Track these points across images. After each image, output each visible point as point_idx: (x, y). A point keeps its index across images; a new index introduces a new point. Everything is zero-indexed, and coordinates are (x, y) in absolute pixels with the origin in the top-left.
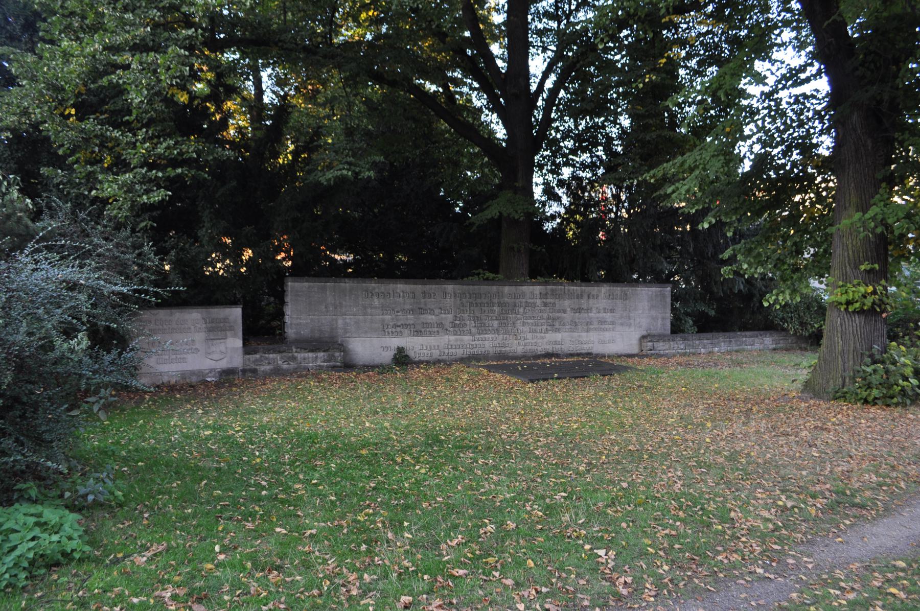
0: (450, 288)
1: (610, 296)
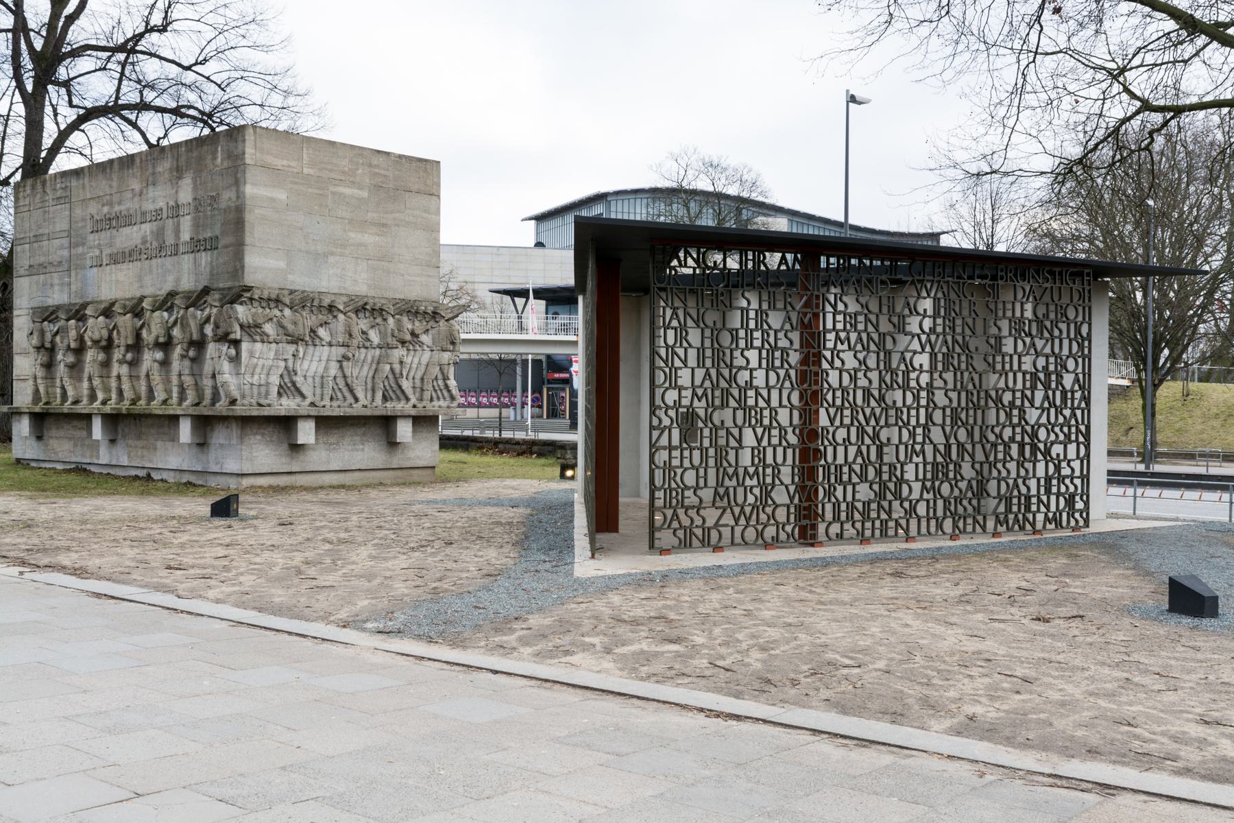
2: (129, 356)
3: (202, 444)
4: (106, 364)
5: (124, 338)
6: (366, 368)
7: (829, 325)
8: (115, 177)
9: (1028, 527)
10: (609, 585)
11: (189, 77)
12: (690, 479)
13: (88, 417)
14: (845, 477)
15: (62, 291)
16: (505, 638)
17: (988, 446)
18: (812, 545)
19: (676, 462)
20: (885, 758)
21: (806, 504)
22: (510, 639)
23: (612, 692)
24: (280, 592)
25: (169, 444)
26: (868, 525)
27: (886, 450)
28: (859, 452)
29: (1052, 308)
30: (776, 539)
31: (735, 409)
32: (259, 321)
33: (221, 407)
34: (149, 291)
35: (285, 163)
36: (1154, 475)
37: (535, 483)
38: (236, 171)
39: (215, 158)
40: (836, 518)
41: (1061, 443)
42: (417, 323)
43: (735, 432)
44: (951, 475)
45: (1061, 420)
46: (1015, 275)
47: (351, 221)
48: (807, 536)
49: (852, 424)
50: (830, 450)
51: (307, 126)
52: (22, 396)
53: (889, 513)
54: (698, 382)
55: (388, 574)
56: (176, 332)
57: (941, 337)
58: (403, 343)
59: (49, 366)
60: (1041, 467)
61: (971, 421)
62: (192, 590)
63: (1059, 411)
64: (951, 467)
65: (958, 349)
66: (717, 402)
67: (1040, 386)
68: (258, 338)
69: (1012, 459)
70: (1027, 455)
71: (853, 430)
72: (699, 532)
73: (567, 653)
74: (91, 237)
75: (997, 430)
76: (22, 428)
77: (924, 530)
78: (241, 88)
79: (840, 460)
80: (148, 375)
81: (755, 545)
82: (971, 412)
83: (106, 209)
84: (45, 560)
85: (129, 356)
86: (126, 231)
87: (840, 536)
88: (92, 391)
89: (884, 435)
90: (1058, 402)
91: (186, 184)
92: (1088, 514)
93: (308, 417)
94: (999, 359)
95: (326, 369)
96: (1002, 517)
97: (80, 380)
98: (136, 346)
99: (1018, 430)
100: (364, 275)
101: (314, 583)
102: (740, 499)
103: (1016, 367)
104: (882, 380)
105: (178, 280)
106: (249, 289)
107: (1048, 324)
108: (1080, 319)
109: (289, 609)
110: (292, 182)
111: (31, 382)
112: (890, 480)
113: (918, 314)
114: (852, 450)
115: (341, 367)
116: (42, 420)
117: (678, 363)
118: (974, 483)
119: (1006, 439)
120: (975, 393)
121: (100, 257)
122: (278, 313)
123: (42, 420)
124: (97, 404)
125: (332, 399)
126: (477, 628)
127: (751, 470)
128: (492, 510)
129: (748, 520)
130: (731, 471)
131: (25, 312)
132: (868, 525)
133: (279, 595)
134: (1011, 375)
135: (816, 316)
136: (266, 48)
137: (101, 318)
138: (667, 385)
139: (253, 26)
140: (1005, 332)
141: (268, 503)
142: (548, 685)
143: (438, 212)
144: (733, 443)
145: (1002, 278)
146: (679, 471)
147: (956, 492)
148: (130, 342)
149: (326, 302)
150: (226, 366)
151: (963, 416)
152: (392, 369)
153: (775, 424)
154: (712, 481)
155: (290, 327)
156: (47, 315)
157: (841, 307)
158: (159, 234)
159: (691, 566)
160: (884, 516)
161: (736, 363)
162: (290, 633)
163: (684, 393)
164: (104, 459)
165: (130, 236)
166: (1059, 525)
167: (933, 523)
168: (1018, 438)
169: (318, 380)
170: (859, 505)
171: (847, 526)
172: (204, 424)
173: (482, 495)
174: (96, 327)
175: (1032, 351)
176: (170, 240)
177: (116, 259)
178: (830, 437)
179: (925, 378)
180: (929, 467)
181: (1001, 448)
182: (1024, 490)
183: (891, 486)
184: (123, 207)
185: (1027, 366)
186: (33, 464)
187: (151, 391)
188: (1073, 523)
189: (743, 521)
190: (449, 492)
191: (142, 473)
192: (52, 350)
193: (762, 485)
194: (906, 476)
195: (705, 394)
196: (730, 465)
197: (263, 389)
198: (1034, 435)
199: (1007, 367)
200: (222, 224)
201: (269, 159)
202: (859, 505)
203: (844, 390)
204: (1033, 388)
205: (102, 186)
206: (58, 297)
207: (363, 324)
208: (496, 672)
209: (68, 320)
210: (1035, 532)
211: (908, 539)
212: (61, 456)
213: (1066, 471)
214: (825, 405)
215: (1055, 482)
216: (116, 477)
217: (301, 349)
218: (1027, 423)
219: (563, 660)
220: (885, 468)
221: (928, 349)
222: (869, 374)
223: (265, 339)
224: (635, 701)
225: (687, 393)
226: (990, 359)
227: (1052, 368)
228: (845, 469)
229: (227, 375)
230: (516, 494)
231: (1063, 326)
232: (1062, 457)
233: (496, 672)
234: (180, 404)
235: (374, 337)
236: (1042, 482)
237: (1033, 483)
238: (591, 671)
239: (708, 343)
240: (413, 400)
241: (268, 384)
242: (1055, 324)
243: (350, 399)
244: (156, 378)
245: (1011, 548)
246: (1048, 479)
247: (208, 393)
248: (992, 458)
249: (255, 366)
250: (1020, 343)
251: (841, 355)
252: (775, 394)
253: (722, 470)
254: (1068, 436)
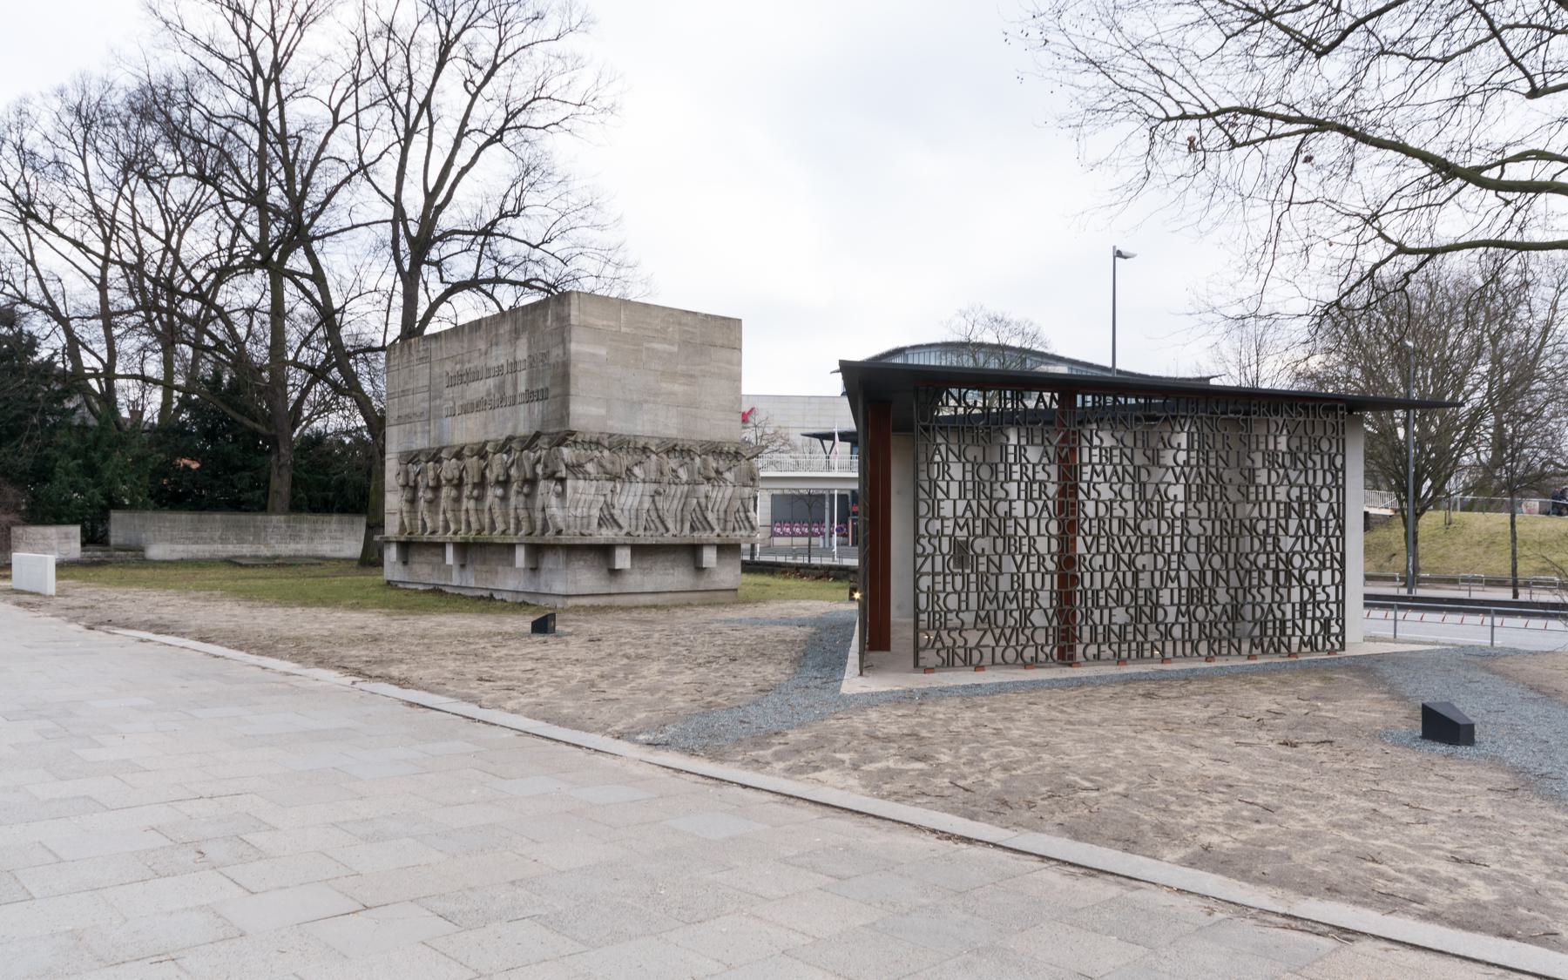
0: (218, 516)
1: (340, 522)
2: (475, 493)
3: (534, 569)
4: (458, 500)
5: (471, 478)
6: (676, 502)
7: (1086, 459)
8: (466, 339)
9: (1283, 649)
10: (871, 701)
11: (537, 254)
12: (952, 602)
13: (442, 545)
14: (1102, 602)
15: (423, 438)
16: (761, 753)
17: (1242, 573)
18: (1070, 665)
19: (939, 587)
20: (1112, 890)
21: (1064, 627)
22: (766, 754)
23: (851, 810)
24: (570, 704)
25: (508, 569)
26: (1124, 647)
27: (1141, 576)
28: (1115, 577)
29: (1306, 440)
30: (1035, 659)
31: (995, 538)
32: (583, 461)
33: (550, 537)
34: (492, 436)
35: (605, 323)
36: (1415, 599)
37: (826, 604)
38: (563, 331)
39: (546, 321)
40: (1093, 640)
41: (1315, 569)
42: (721, 462)
43: (996, 559)
44: (1206, 600)
45: (1315, 547)
46: (1269, 411)
47: (663, 373)
48: (1066, 656)
49: (1108, 551)
50: (1087, 577)
51: (636, 294)
52: (392, 528)
53: (1145, 636)
54: (959, 512)
55: (670, 688)
56: (513, 471)
57: (1195, 469)
58: (709, 479)
59: (413, 501)
60: (1295, 595)
61: (1225, 548)
62: (494, 701)
63: (1313, 539)
64: (1206, 592)
65: (1212, 481)
66: (979, 531)
67: (1294, 515)
68: (581, 476)
69: (1266, 585)
70: (1282, 580)
71: (1110, 558)
72: (961, 652)
73: (817, 769)
74: (447, 391)
75: (1252, 557)
76: (391, 554)
77: (1179, 651)
78: (580, 262)
79: (1098, 585)
80: (490, 509)
81: (1014, 664)
82: (1225, 540)
83: (458, 367)
84: (378, 672)
85: (475, 493)
86: (474, 385)
87: (1097, 657)
88: (447, 522)
89: (1140, 561)
90: (1312, 531)
91: (523, 343)
92: (1344, 638)
93: (624, 545)
94: (1252, 489)
95: (641, 502)
96: (1257, 641)
97: (437, 513)
98: (481, 484)
99: (1273, 557)
100: (674, 420)
101: (603, 695)
102: (1000, 621)
103: (1269, 497)
104: (1137, 510)
105: (515, 427)
106: (573, 433)
107: (1302, 456)
108: (1334, 450)
109: (574, 720)
110: (611, 340)
111: (398, 516)
112: (1146, 604)
113: (1172, 447)
114: (1109, 576)
115: (654, 501)
116: (407, 548)
117: (940, 495)
118: (1229, 608)
119: (1261, 566)
120: (1229, 521)
121: (453, 408)
122: (598, 454)
123: (407, 548)
124: (450, 534)
125: (645, 529)
126: (739, 741)
127: (1011, 595)
128: (780, 629)
129: (1008, 641)
130: (991, 595)
131: (394, 456)
132: (1124, 647)
133: (568, 707)
134: (1265, 505)
135: (1073, 450)
136: (601, 227)
137: (454, 460)
138: (930, 515)
139: (590, 209)
140: (1259, 464)
141: (587, 622)
142: (792, 800)
143: (739, 364)
144: (993, 569)
145: (1255, 413)
146: (942, 596)
147: (1211, 616)
148: (476, 480)
149: (641, 444)
150: (554, 501)
151: (1217, 544)
152: (698, 503)
153: (1033, 551)
154: (973, 605)
155: (609, 466)
156: (410, 458)
157: (1096, 441)
158: (501, 387)
159: (952, 684)
160: (1140, 638)
161: (995, 495)
162: (568, 744)
163: (946, 523)
164: (455, 583)
165: (478, 390)
166: (1314, 647)
167: (1188, 645)
168: (1273, 565)
169: (633, 512)
170: (1116, 628)
171: (1104, 648)
172: (537, 551)
173: (776, 615)
174: (449, 468)
175: (1286, 482)
176: (509, 392)
177: (466, 409)
178: (1087, 563)
179: (1179, 508)
180: (1184, 593)
181: (1255, 574)
182: (1279, 614)
183: (1147, 610)
184: (471, 365)
185: (1281, 496)
186: (400, 585)
187: (493, 522)
188: (1328, 646)
189: (1002, 642)
190: (747, 612)
191: (486, 594)
192: (415, 488)
193: (1021, 609)
194: (1161, 601)
195: (966, 524)
196: (991, 590)
197: (585, 521)
198: (1289, 562)
199: (1261, 497)
201: (591, 320)
202: (1116, 628)
203: (1100, 519)
204: (1287, 517)
205: (455, 347)
206: (420, 443)
207: (673, 463)
208: (745, 787)
209: (427, 462)
210: (1290, 654)
211: (1164, 660)
212: (422, 579)
213: (1321, 597)
214: (1082, 533)
215: (1310, 607)
216: (465, 597)
217: (618, 486)
218: (1281, 551)
219: (811, 776)
220: (1141, 593)
221: (1182, 480)
222: (1124, 505)
223: (587, 477)
224: (871, 820)
225: (950, 523)
226: (1243, 490)
227: (1306, 498)
228: (1102, 594)
229: (555, 509)
230: (805, 614)
231: (1317, 458)
232: (1317, 583)
233: (745, 787)
234: (516, 534)
235: (683, 474)
236: (1297, 607)
237: (1288, 608)
238: (836, 788)
239: (969, 476)
240: (717, 530)
241: (589, 516)
242: (1309, 455)
243: (662, 530)
244: (497, 512)
245: (1267, 670)
246: (1303, 604)
247: (539, 524)
248: (1247, 584)
249: (578, 501)
250: (1273, 474)
251: (1097, 487)
252: (1033, 523)
253: (982, 595)
254: (1323, 563)
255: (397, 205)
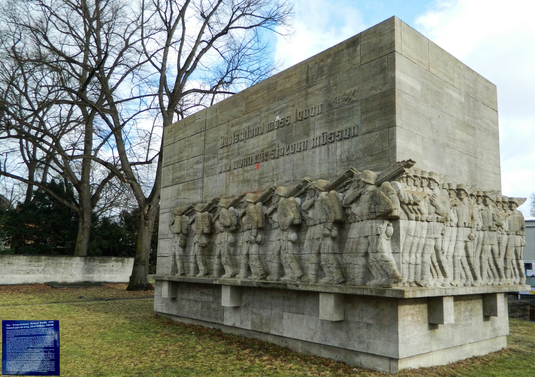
2: (259, 237)
13: (218, 288)
68: (413, 216)
74: (221, 151)
85: (259, 237)
111: (171, 259)
137: (232, 208)
200: (363, 113)
234: (317, 281)
255: (162, 70)
